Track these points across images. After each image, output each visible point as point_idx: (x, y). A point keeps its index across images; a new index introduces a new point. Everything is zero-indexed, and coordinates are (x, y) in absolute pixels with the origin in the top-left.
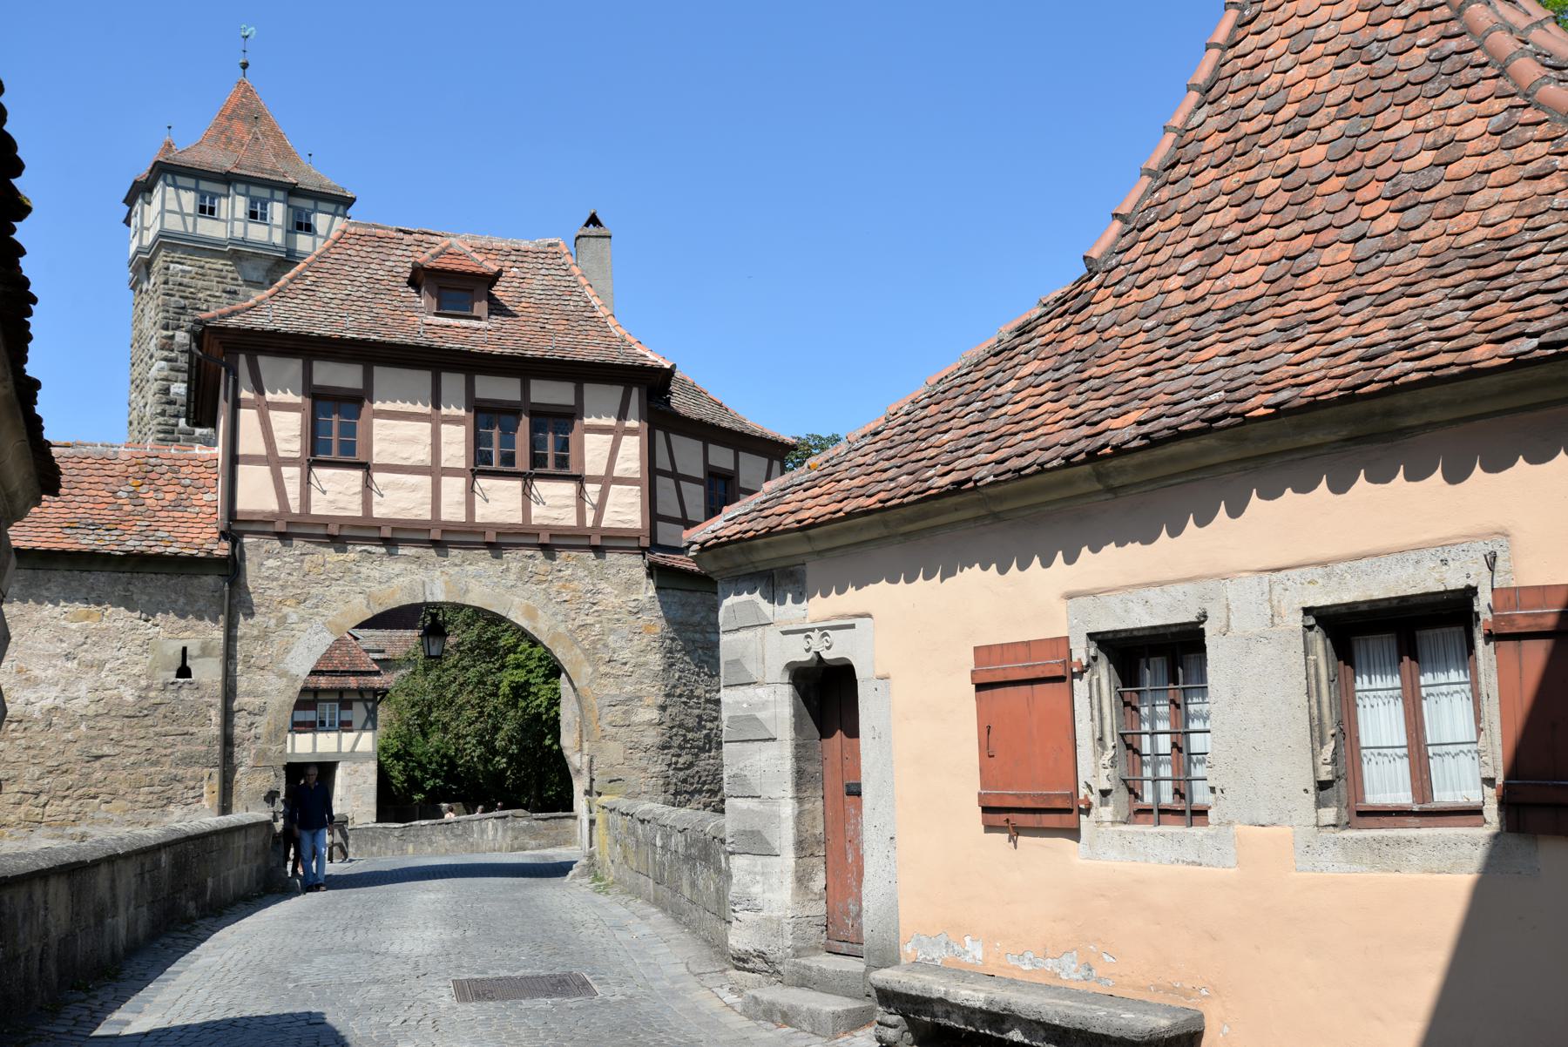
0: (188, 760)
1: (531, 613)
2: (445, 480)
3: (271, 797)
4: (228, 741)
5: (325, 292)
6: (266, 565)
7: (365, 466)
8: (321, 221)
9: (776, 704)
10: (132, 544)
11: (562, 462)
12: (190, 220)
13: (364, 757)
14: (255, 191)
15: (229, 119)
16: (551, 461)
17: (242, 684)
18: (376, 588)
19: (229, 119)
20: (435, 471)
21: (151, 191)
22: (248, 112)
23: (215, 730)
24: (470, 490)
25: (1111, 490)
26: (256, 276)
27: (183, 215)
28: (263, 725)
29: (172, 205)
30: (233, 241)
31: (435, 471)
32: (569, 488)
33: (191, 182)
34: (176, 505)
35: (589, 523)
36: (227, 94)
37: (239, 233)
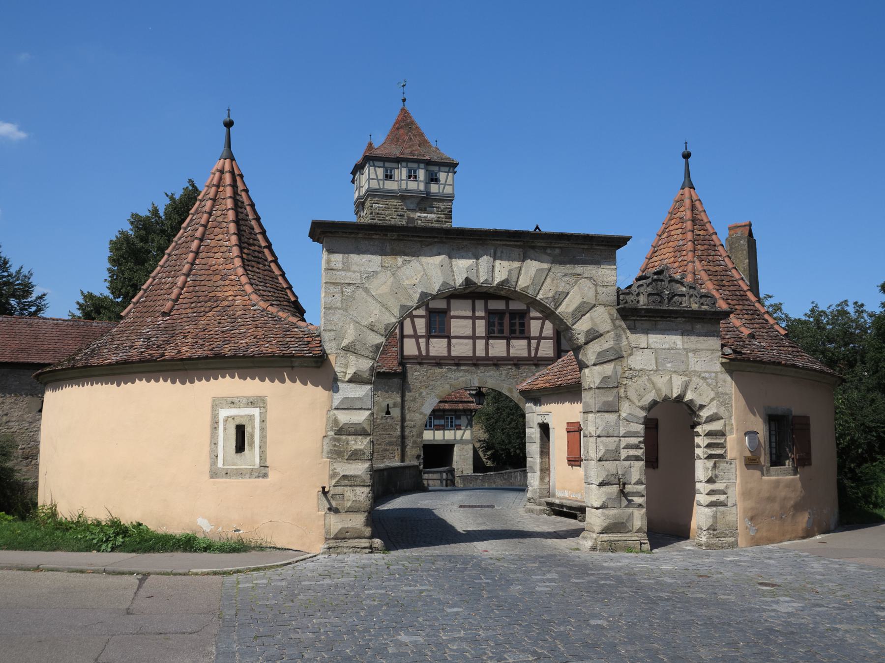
0: (390, 444)
3: (418, 457)
4: (403, 437)
6: (415, 374)
7: (449, 338)
8: (442, 176)
11: (522, 332)
12: (381, 182)
13: (466, 442)
14: (411, 165)
15: (398, 129)
16: (517, 332)
17: (408, 417)
18: (453, 382)
19: (398, 129)
20: (474, 338)
21: (363, 168)
22: (405, 124)
23: (399, 433)
24: (487, 344)
26: (412, 206)
27: (378, 180)
28: (415, 432)
29: (373, 176)
30: (401, 190)
31: (474, 338)
32: (524, 342)
33: (381, 164)
35: (533, 355)
36: (395, 114)
37: (404, 187)
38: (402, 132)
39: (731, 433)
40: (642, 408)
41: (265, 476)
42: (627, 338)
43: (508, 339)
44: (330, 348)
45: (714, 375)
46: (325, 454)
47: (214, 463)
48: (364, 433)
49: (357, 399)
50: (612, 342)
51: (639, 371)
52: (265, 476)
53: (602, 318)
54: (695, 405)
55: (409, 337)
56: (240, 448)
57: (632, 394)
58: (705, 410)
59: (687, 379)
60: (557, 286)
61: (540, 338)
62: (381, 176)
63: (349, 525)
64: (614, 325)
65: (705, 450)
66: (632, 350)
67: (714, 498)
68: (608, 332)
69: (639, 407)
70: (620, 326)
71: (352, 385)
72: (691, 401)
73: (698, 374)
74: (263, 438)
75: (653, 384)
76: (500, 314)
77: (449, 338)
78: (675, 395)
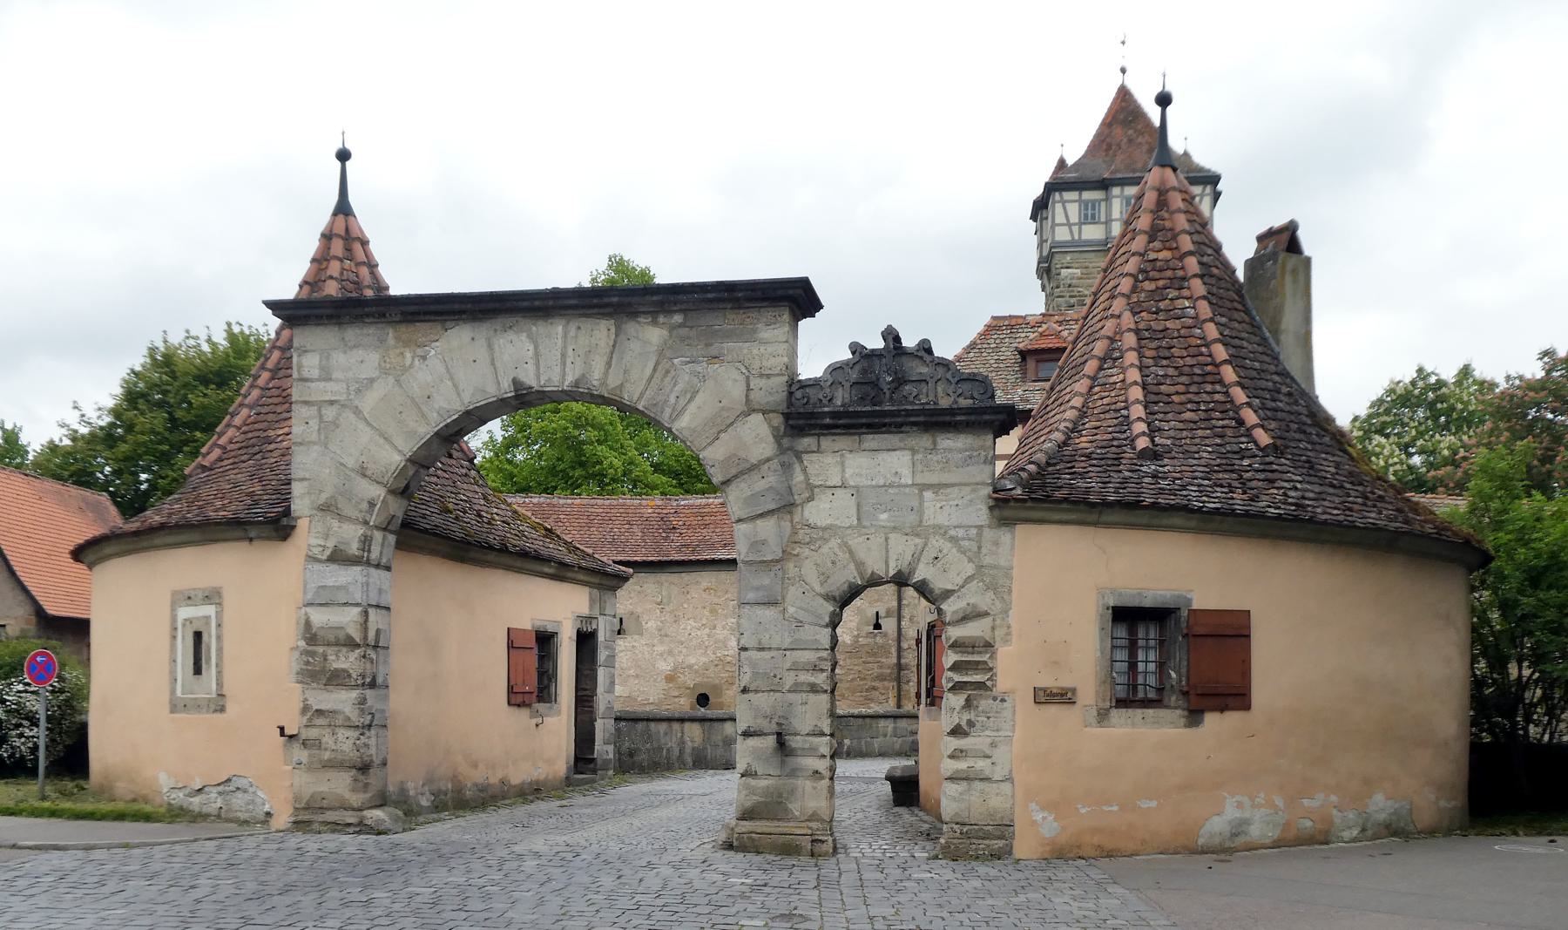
12: (1075, 229)
27: (1069, 225)
33: (1073, 195)
38: (1118, 131)
41: (222, 709)
42: (804, 470)
44: (301, 504)
45: (974, 531)
46: (293, 677)
47: (173, 691)
48: (351, 644)
49: (339, 588)
51: (824, 529)
52: (222, 709)
53: (757, 437)
56: (198, 670)
57: (810, 571)
62: (1074, 218)
63: (323, 788)
64: (779, 444)
66: (812, 492)
67: (962, 765)
68: (768, 460)
71: (333, 567)
73: (942, 531)
74: (220, 650)
75: (851, 552)
78: (892, 573)
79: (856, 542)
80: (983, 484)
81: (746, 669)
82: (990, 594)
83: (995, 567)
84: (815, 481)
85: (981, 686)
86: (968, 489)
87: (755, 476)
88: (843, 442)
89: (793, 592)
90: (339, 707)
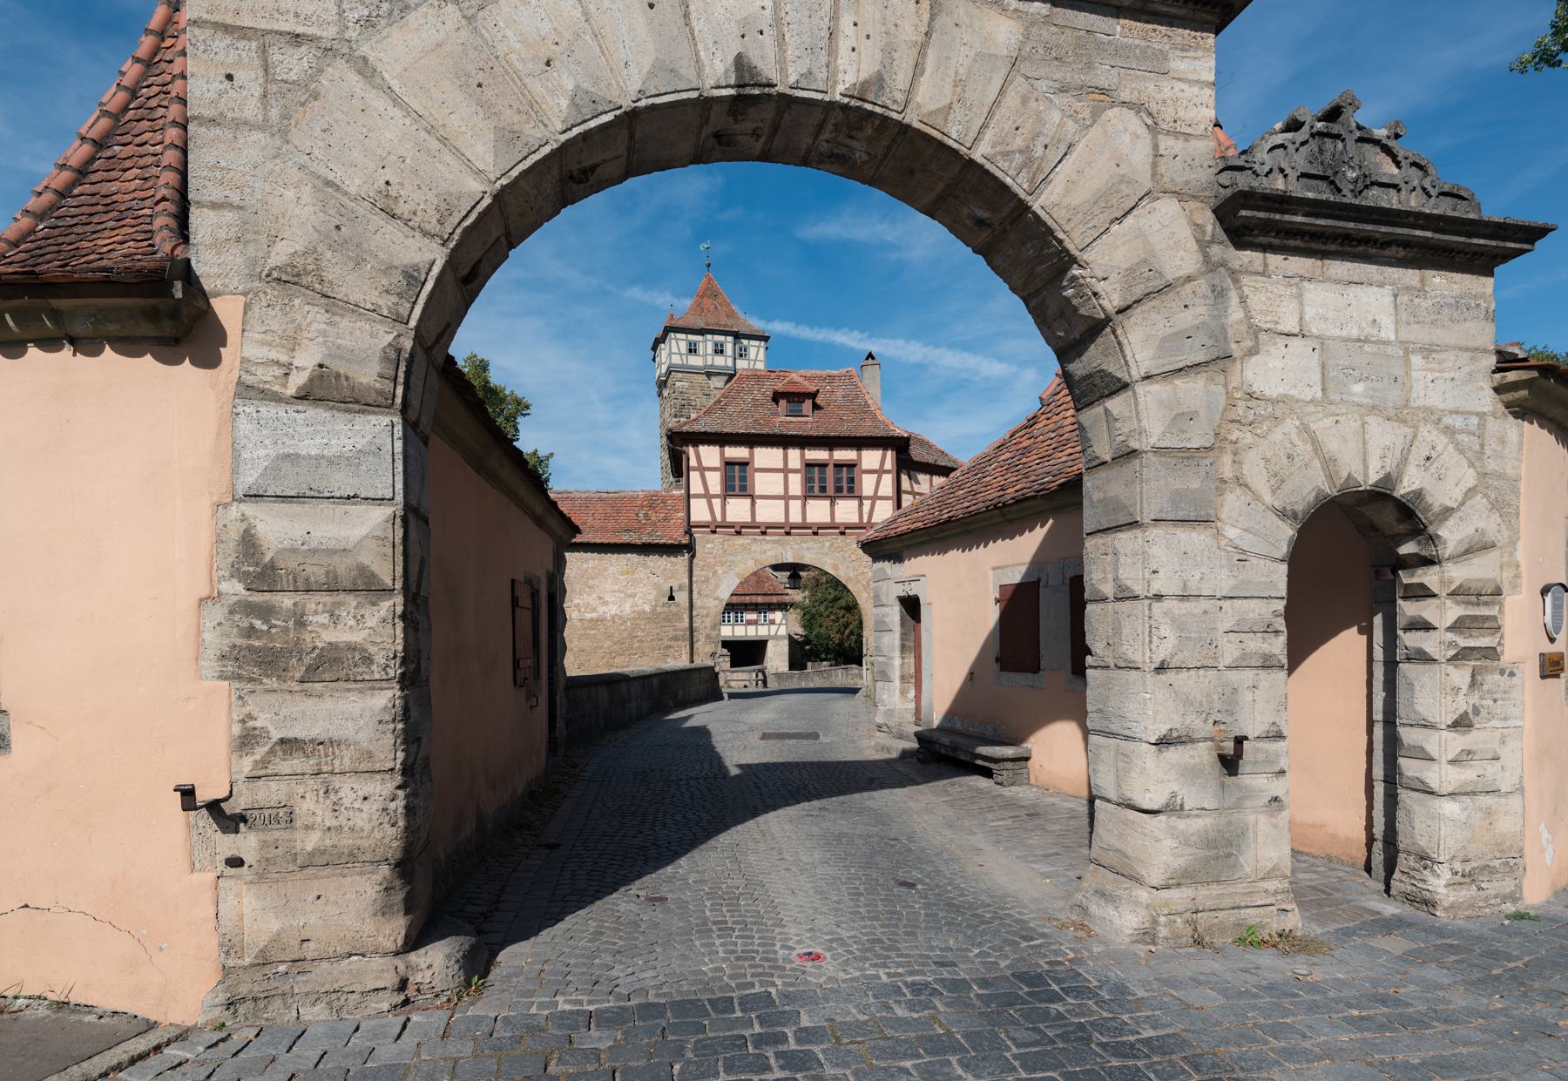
0: (676, 638)
1: (836, 567)
2: (791, 502)
5: (730, 409)
6: (706, 545)
7: (752, 497)
9: (894, 614)
10: (645, 539)
11: (851, 490)
13: (782, 638)
17: (697, 602)
18: (759, 556)
20: (786, 497)
24: (804, 506)
25: (1010, 521)
28: (708, 622)
31: (786, 497)
32: (855, 503)
34: (665, 519)
39: (1515, 587)
40: (1283, 514)
42: (1243, 301)
43: (833, 499)
45: (1475, 420)
50: (1202, 309)
54: (1428, 508)
55: (698, 496)
58: (1451, 522)
59: (1408, 431)
60: (1040, 119)
61: (875, 498)
65: (1450, 636)
68: (1189, 279)
69: (1275, 510)
70: (1224, 264)
72: (1419, 494)
73: (1432, 416)
76: (823, 465)
77: (752, 497)
78: (1373, 478)
79: (1321, 425)
80: (1485, 351)
81: (1165, 630)
82: (1496, 517)
83: (1500, 476)
84: (1260, 320)
85: (1491, 653)
86: (1467, 355)
87: (1171, 302)
88: (1299, 264)
89: (1232, 503)
90: (347, 731)
